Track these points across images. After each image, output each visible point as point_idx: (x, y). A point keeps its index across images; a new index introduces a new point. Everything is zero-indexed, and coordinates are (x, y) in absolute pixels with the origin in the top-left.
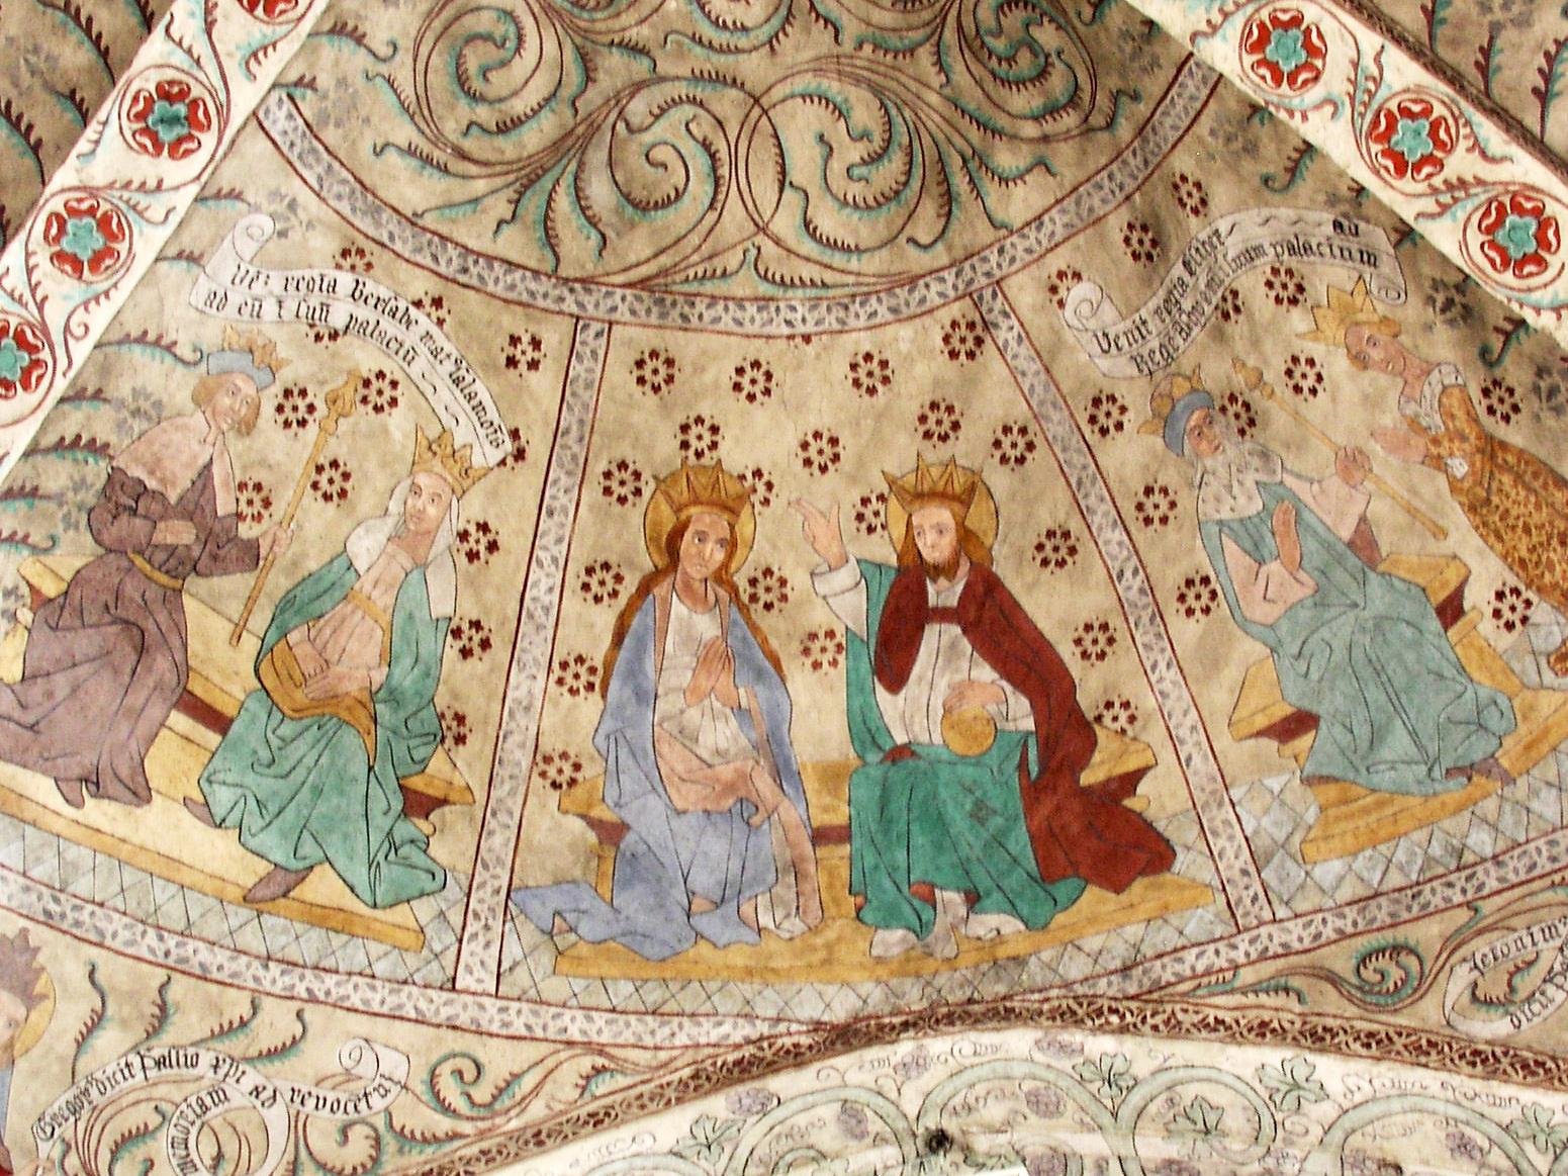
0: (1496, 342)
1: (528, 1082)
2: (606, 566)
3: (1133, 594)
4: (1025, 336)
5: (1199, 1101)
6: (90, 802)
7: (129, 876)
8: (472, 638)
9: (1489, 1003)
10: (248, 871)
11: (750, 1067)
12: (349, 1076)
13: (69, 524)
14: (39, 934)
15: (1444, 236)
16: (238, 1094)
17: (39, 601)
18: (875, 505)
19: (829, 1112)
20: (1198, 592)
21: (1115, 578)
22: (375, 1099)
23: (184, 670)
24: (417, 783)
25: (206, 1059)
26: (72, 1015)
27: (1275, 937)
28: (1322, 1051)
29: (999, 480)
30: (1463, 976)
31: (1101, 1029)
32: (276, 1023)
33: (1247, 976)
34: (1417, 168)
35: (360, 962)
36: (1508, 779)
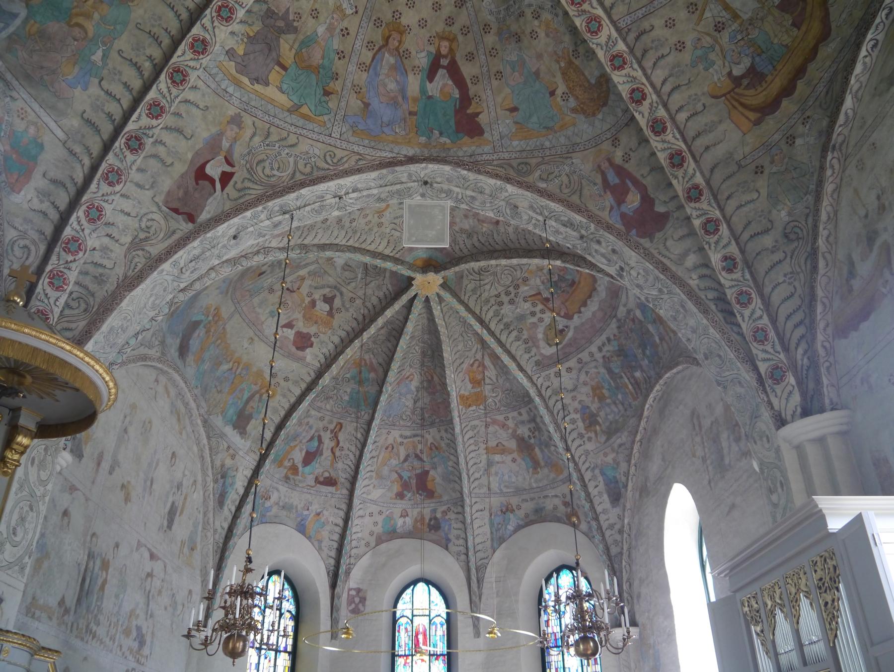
0: (579, 42)
1: (345, 159)
2: (372, 42)
3: (485, 71)
4: (473, 6)
5: (481, 187)
6: (256, 84)
7: (263, 102)
8: (341, 55)
9: (543, 179)
10: (289, 104)
11: (391, 164)
12: (307, 153)
13: (257, 19)
14: (243, 113)
15: (578, 22)
16: (284, 154)
17: (249, 37)
18: (432, 38)
19: (405, 175)
20: (499, 74)
21: (481, 67)
22: (313, 159)
23: (279, 56)
24: (327, 88)
25: (277, 145)
26: (249, 132)
27: (502, 155)
28: (509, 183)
29: (460, 38)
30: (537, 173)
31: (464, 169)
32: (292, 139)
33: (495, 163)
34: (576, 4)
35: (311, 128)
36: (556, 132)
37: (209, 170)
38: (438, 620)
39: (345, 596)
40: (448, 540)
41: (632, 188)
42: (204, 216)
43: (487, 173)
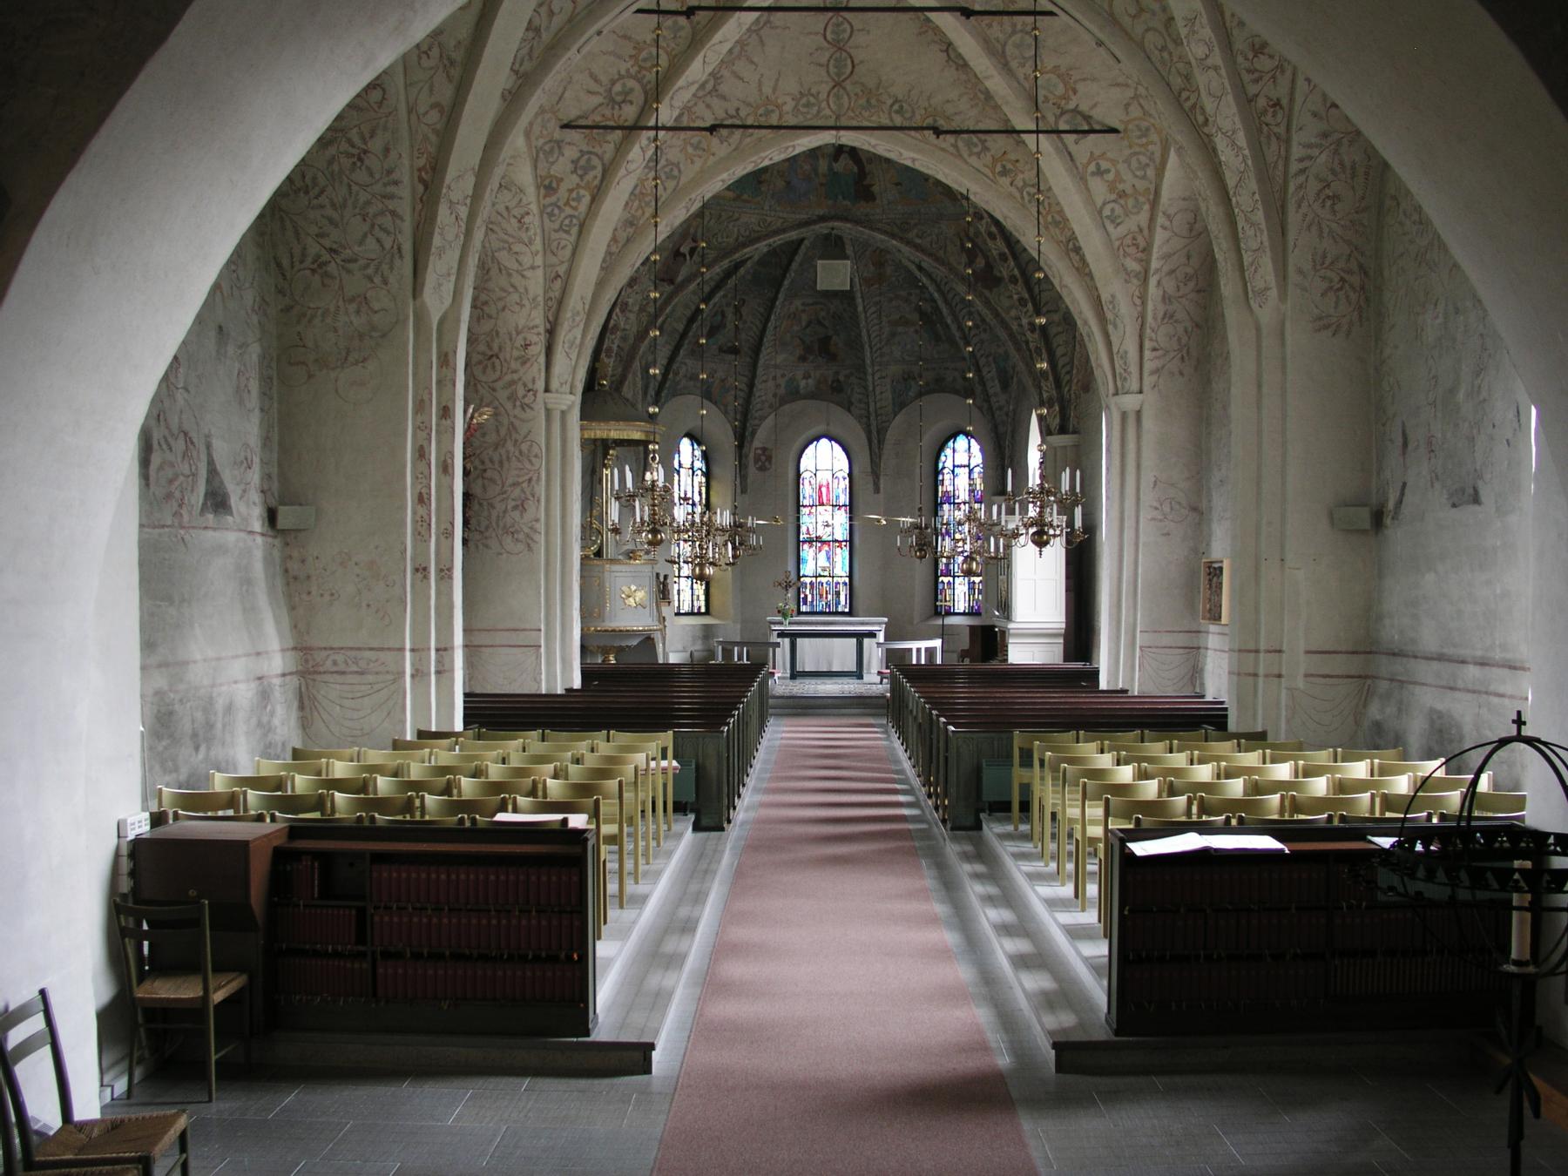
16: (731, 227)
30: (915, 231)
32: (736, 215)
37: (682, 250)
38: (840, 475)
39: (752, 455)
40: (851, 403)
41: (980, 254)
42: (679, 279)
43: (878, 230)
